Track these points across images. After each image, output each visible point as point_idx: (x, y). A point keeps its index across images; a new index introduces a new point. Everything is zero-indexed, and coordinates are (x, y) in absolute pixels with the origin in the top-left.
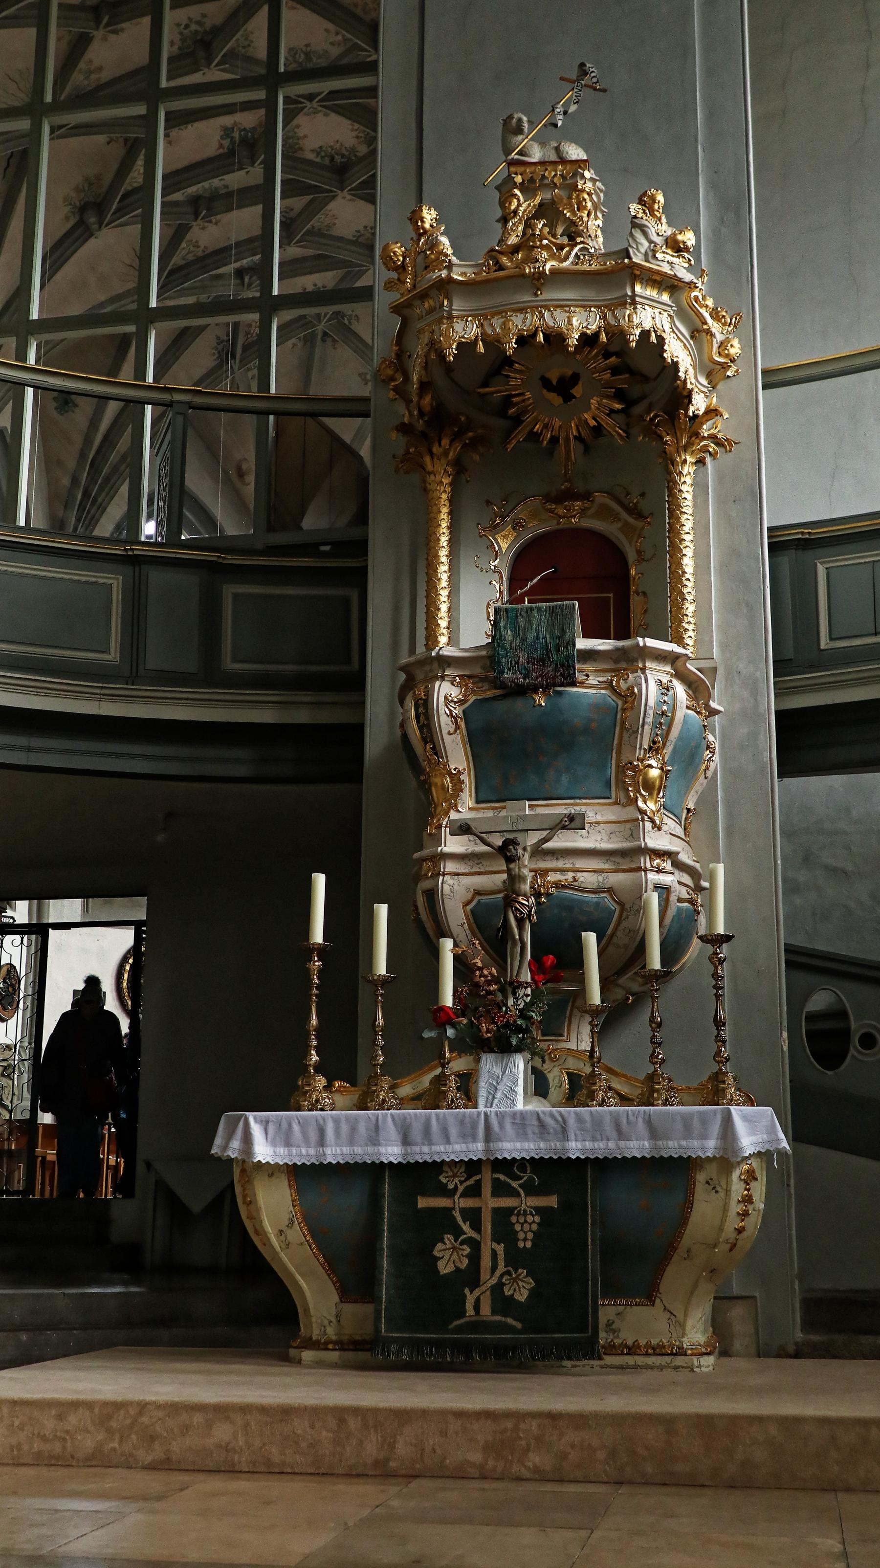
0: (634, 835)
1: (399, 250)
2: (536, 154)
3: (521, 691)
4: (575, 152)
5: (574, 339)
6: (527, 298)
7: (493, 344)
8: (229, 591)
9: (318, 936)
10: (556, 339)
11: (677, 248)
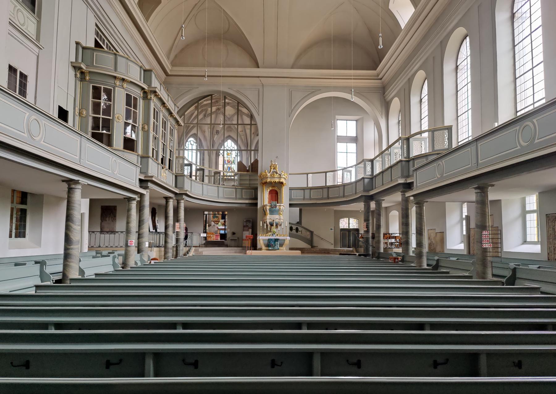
0: (280, 218)
1: (264, 173)
2: (273, 164)
3: (273, 208)
4: (276, 164)
5: (277, 182)
6: (273, 178)
7: (271, 182)
8: (243, 190)
9: (261, 225)
10: (276, 182)
11: (284, 175)
